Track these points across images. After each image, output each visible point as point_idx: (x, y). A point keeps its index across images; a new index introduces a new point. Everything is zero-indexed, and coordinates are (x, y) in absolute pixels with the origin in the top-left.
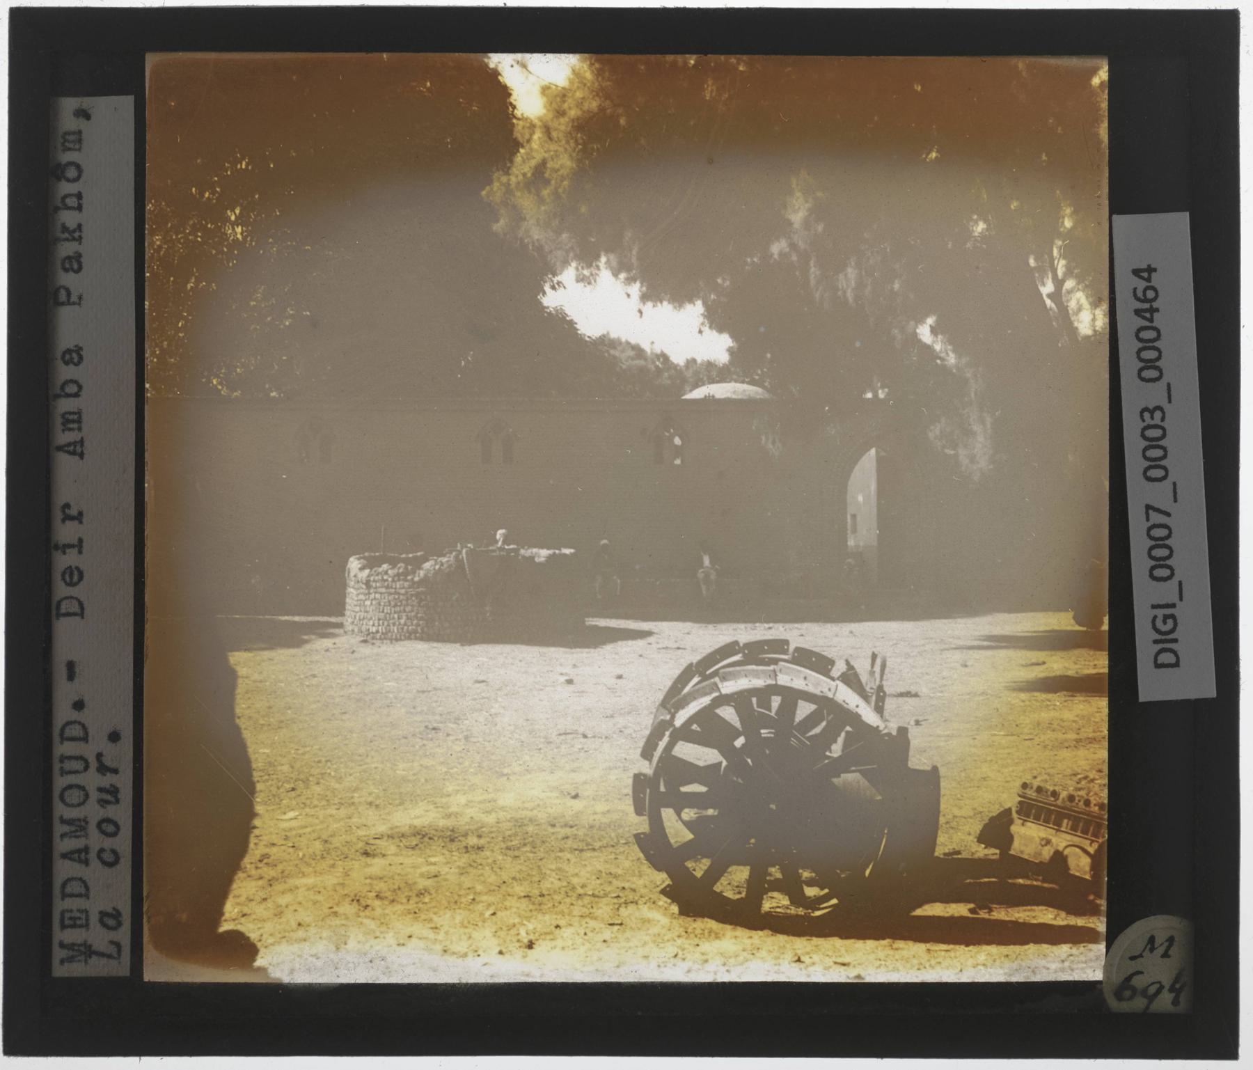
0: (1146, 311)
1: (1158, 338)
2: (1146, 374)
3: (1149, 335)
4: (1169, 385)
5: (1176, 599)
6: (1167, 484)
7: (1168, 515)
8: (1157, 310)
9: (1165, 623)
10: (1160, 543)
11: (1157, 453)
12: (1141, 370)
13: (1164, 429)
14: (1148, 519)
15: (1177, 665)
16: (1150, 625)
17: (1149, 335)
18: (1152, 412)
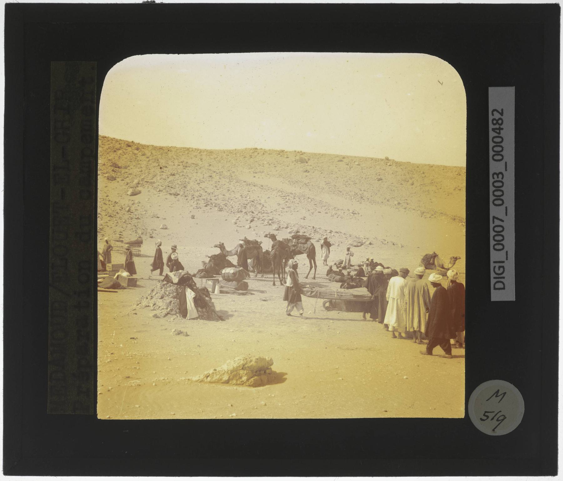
0: (496, 129)
2: (496, 158)
3: (499, 140)
4: (506, 163)
5: (504, 259)
6: (503, 207)
7: (503, 221)
8: (502, 129)
9: (499, 270)
12: (494, 156)
14: (493, 223)
15: (504, 288)
17: (499, 140)
18: (498, 175)
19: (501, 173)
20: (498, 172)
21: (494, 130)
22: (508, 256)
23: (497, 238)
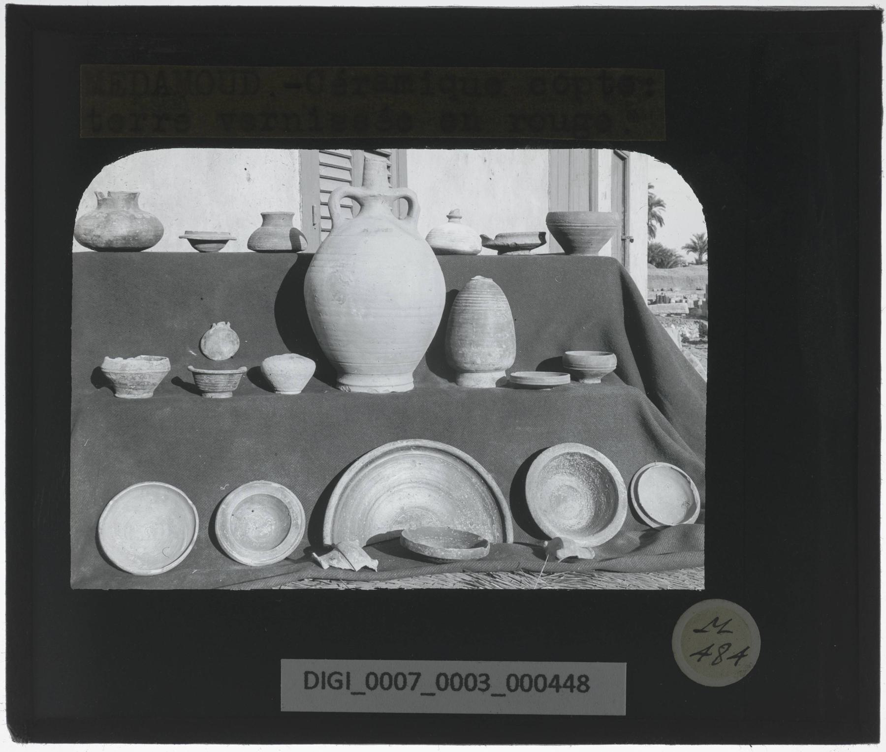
1: (538, 690)
3: (541, 684)
4: (504, 695)
5: (353, 688)
6: (434, 689)
7: (413, 688)
8: (557, 691)
10: (393, 681)
14: (410, 674)
17: (541, 684)
18: (485, 682)
19: (487, 689)
20: (489, 682)
21: (557, 677)
23: (386, 678)
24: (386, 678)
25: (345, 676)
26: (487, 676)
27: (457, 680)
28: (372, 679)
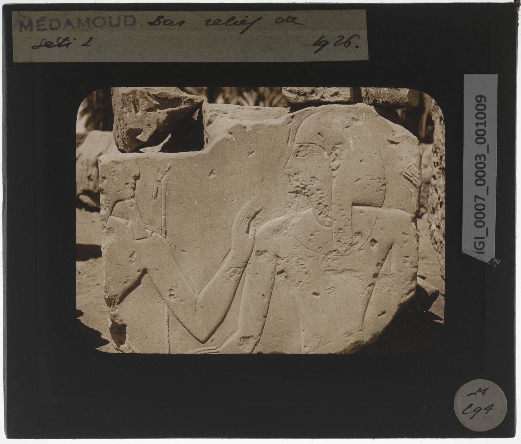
4: (488, 146)
5: (485, 236)
6: (485, 187)
7: (484, 200)
10: (480, 211)
11: (481, 174)
13: (484, 164)
14: (475, 201)
16: (473, 245)
18: (480, 157)
22: (488, 232)
23: (478, 216)
24: (478, 216)
25: (476, 240)
26: (477, 155)
27: (481, 174)
28: (479, 224)
